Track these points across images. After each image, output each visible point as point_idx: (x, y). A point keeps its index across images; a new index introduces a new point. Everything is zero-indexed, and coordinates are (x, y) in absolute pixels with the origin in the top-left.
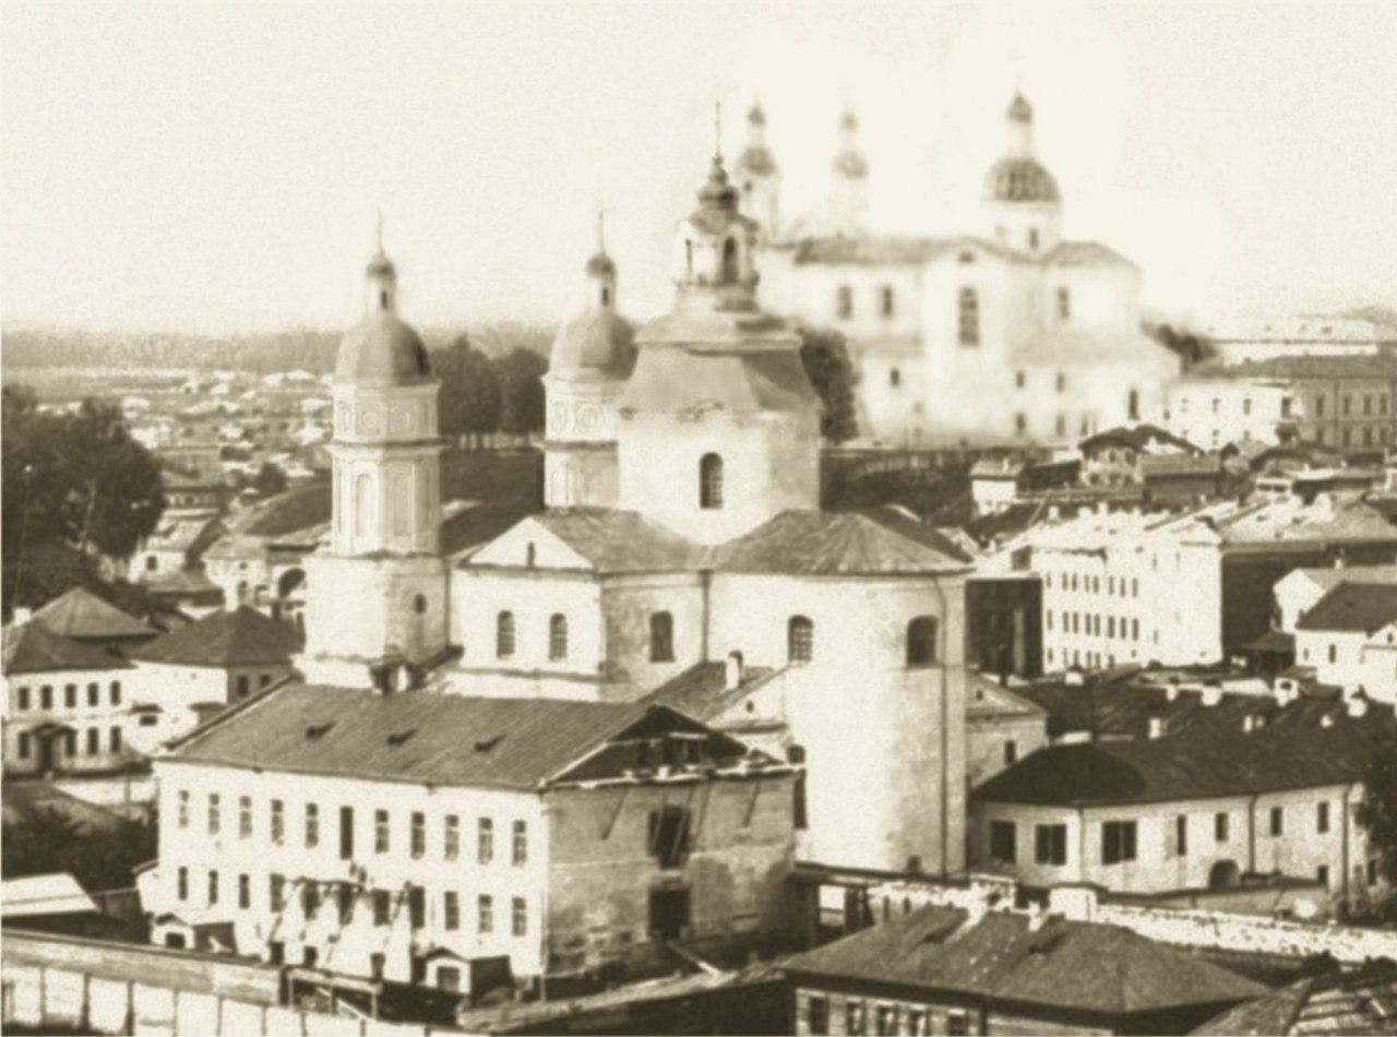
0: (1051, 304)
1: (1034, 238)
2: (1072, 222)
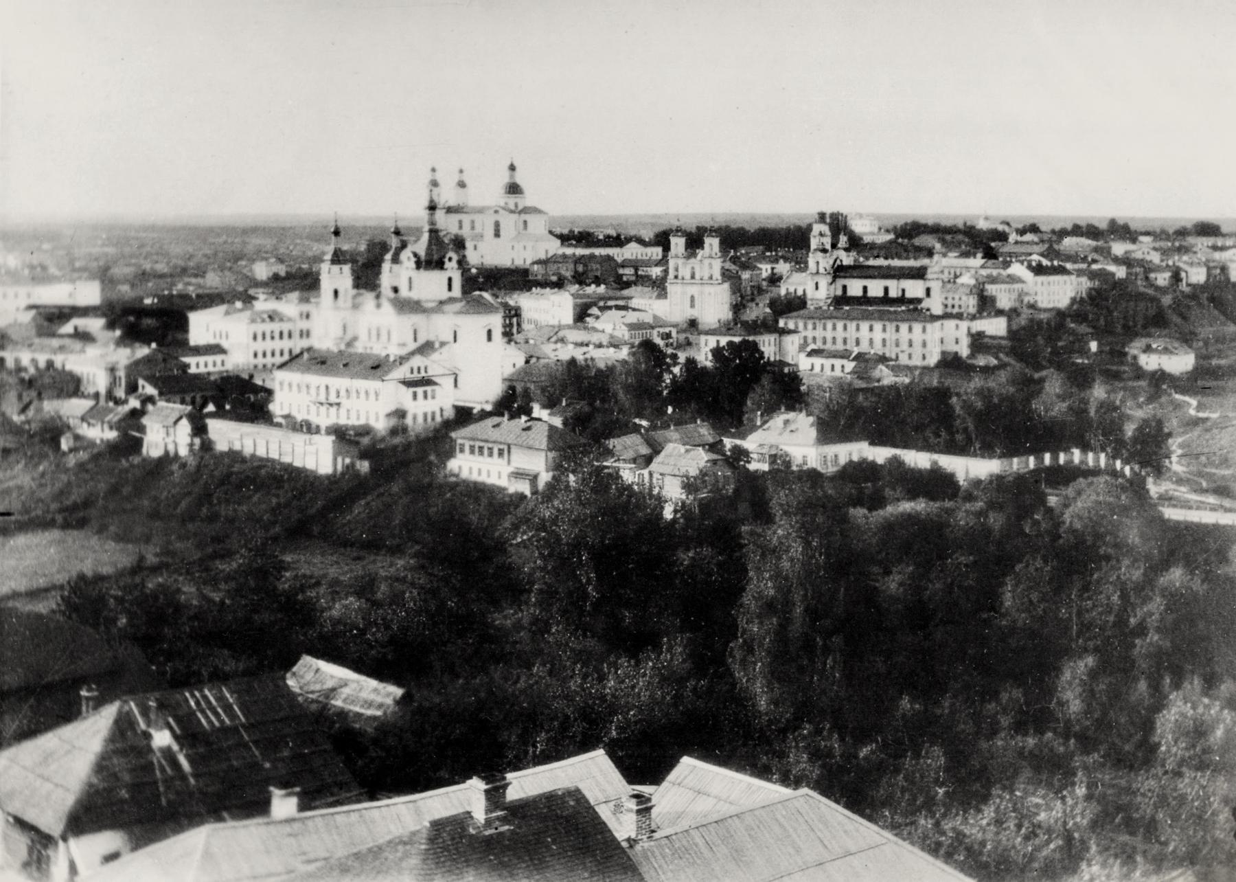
0: (521, 226)
1: (516, 205)
2: (528, 200)
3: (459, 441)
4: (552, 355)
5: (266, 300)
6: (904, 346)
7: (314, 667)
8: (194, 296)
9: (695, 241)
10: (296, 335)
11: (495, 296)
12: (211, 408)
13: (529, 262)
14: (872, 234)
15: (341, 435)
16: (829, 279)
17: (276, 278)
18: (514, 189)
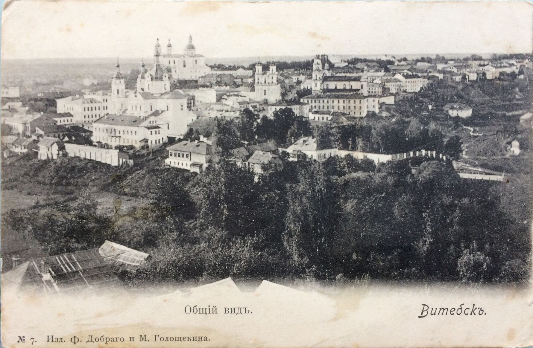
0: (195, 62)
1: (192, 54)
2: (197, 52)
3: (170, 151)
4: (208, 115)
5: (89, 94)
6: (352, 109)
7: (111, 246)
8: (58, 93)
9: (266, 68)
10: (102, 108)
11: (184, 91)
12: (66, 139)
13: (198, 77)
14: (338, 63)
15: (120, 149)
16: (321, 82)
17: (93, 85)
18: (191, 47)
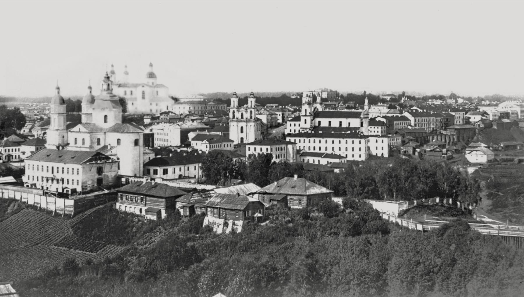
0: (155, 93)
1: (153, 84)
2: (158, 81)
6: (349, 149)
9: (243, 102)
16: (312, 117)
18: (152, 75)
